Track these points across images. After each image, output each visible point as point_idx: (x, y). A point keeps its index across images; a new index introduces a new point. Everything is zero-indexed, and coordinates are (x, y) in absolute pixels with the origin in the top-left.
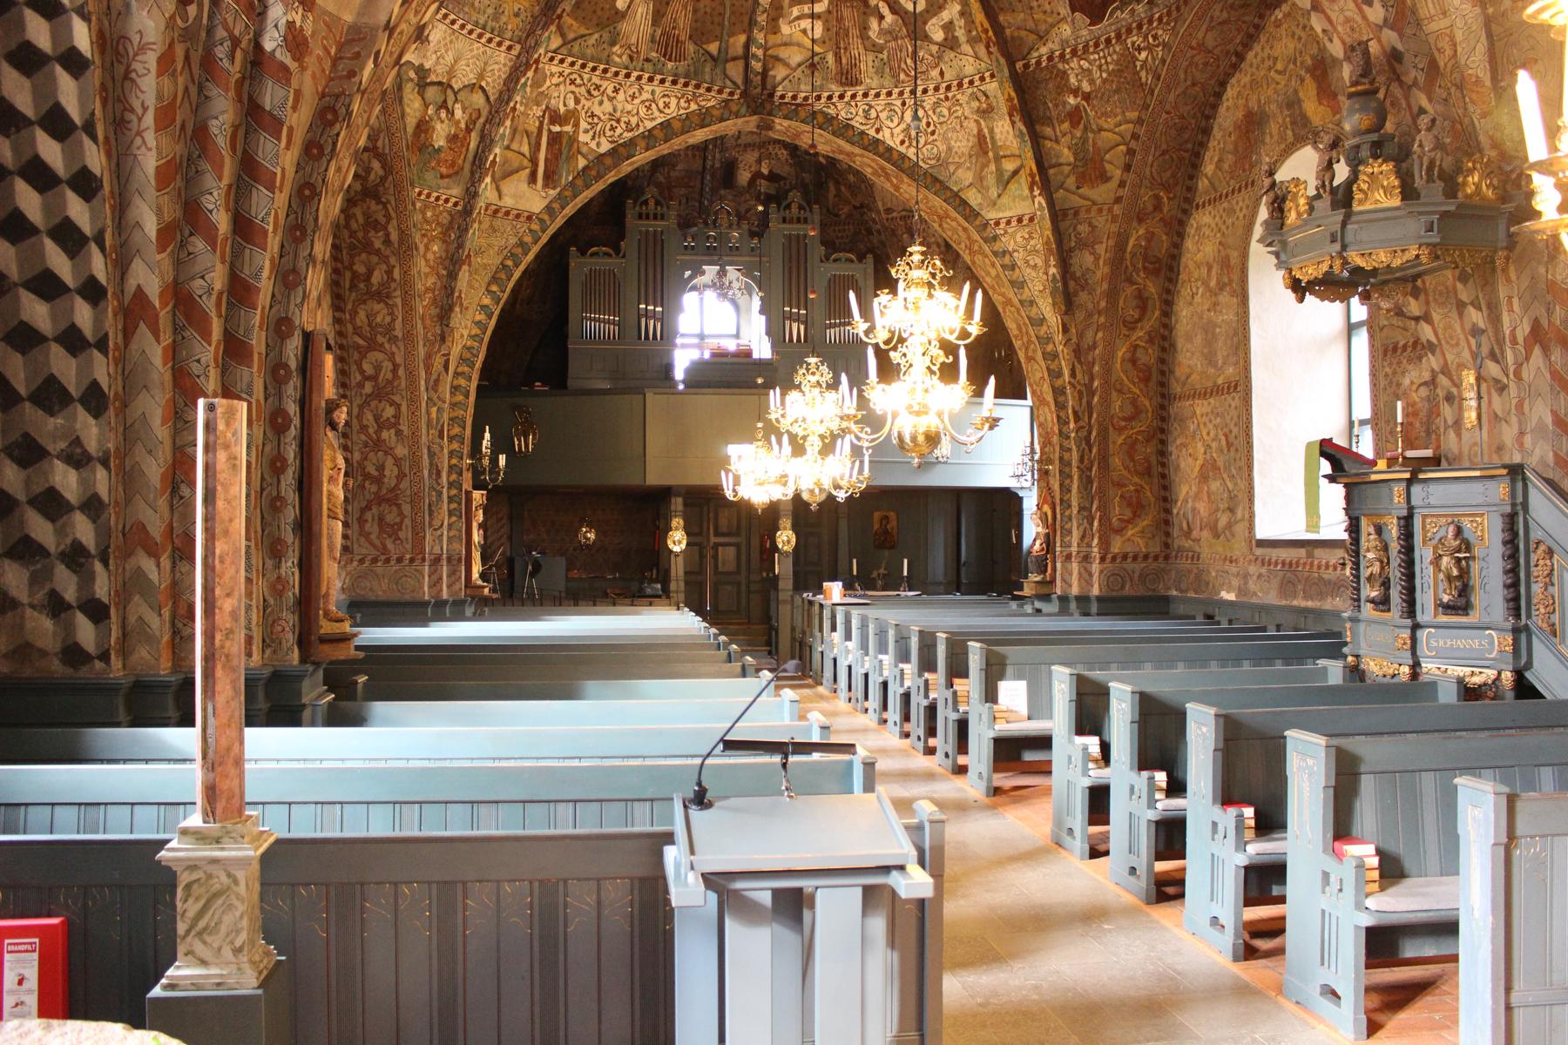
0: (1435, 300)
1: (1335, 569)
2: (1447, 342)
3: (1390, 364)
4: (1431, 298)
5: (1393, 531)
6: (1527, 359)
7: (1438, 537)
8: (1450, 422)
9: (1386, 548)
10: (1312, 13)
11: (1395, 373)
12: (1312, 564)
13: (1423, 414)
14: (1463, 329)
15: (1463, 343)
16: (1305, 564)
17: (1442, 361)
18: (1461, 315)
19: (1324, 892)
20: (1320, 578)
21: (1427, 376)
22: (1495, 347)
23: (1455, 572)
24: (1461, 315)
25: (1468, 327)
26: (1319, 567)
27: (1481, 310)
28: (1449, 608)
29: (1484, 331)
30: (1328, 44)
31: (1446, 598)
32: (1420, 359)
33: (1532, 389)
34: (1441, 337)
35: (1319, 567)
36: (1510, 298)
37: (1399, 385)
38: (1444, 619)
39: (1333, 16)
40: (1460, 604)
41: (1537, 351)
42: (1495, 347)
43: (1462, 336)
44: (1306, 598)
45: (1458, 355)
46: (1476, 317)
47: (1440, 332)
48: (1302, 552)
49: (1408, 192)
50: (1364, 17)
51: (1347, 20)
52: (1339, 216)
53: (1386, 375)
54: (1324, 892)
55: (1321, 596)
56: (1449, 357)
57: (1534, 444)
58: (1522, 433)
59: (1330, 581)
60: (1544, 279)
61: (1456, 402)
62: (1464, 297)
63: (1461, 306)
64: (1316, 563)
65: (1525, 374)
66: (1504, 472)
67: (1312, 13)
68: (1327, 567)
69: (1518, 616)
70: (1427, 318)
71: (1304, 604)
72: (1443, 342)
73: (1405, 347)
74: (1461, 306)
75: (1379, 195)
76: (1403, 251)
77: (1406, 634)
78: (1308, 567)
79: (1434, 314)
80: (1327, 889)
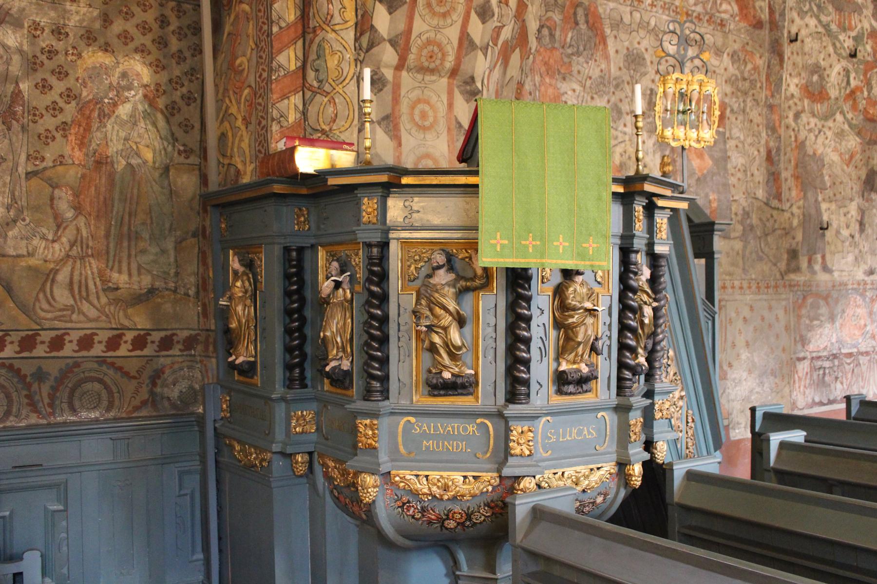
15: (457, 17)
45: (437, 29)
56: (419, 26)
61: (388, 89)
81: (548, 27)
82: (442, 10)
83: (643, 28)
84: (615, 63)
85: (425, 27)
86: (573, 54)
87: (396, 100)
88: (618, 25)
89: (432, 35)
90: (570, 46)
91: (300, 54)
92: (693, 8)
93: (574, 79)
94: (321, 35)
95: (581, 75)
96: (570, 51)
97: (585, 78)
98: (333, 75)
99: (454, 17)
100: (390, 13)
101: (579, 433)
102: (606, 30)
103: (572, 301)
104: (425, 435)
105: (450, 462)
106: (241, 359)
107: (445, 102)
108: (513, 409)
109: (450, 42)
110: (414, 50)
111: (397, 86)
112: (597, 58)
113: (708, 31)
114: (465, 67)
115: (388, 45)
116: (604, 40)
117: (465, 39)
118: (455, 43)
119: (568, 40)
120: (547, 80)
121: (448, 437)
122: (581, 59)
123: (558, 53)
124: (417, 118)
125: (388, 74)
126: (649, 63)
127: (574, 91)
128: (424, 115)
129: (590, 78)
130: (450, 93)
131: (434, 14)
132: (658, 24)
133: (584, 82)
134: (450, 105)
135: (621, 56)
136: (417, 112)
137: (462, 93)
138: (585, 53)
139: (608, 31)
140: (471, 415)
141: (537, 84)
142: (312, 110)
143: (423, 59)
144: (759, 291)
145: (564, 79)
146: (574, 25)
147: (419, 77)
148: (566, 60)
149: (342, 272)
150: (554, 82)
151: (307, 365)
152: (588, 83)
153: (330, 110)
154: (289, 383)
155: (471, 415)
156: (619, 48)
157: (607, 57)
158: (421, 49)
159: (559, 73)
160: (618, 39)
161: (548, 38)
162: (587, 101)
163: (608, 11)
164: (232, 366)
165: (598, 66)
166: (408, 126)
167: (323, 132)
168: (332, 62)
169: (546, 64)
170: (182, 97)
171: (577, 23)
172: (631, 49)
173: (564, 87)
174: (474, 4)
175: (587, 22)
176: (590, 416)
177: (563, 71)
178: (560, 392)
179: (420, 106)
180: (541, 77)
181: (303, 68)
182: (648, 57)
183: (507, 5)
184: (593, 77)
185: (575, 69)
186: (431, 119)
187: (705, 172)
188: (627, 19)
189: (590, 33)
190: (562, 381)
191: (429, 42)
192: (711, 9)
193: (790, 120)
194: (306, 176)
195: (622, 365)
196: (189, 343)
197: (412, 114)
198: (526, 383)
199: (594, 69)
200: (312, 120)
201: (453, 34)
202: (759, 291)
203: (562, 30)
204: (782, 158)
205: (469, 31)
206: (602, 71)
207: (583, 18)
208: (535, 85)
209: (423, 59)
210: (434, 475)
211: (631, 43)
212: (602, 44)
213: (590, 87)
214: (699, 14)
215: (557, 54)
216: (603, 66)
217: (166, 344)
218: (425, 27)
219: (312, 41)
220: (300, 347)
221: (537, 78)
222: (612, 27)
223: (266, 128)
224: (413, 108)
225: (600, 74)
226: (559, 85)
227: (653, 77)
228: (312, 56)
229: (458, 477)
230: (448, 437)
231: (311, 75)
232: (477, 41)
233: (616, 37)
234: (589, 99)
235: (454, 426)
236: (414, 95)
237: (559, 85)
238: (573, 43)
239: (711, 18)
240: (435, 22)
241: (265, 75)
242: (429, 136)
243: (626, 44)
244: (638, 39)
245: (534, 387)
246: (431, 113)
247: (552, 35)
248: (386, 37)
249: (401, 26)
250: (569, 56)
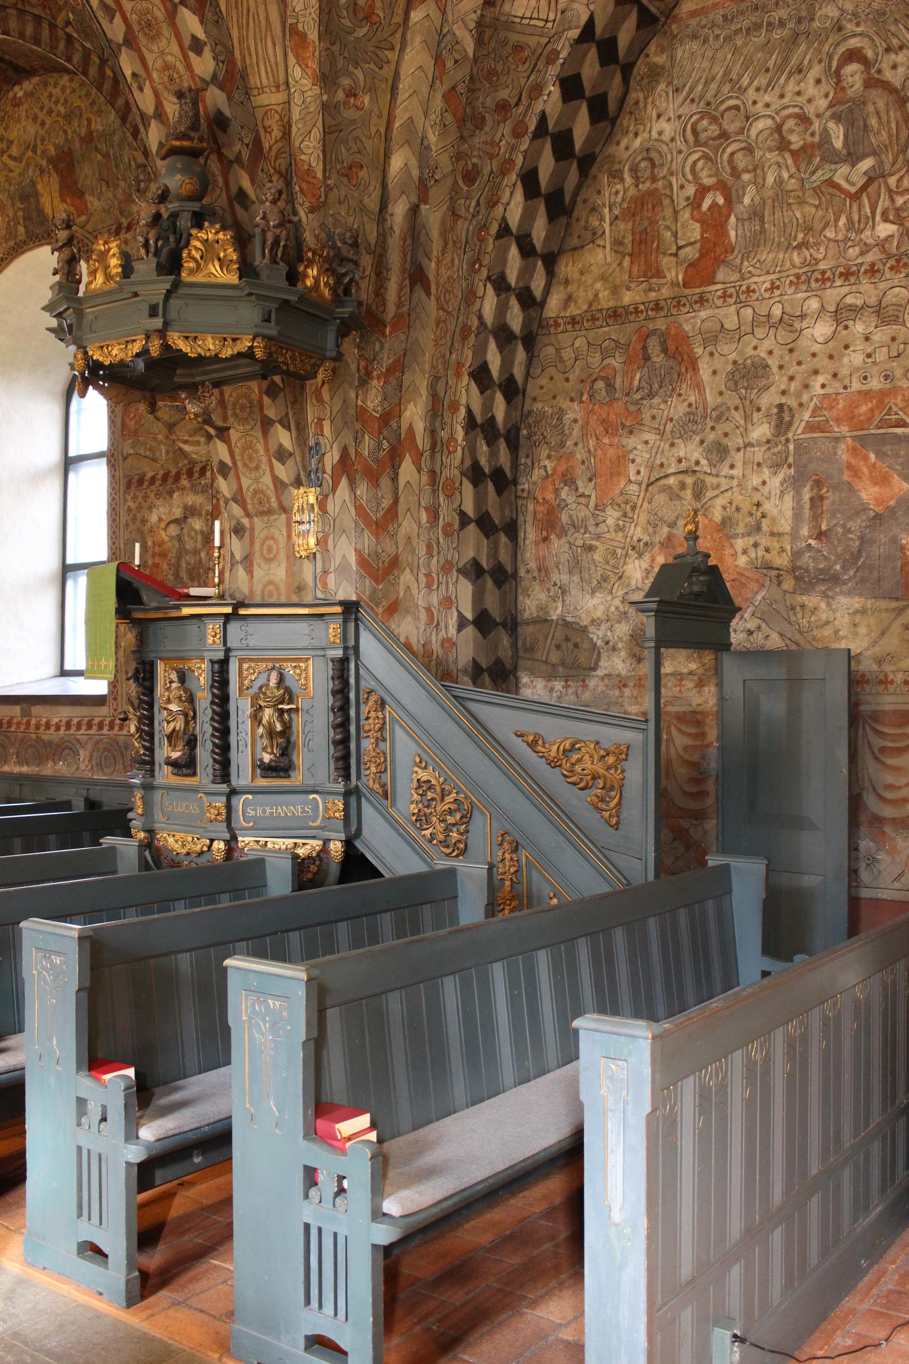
0: (235, 415)
1: (58, 728)
2: (245, 465)
3: (135, 498)
4: (230, 413)
5: (202, 676)
6: (334, 490)
7: (257, 685)
8: (238, 557)
9: (191, 699)
10: (123, 49)
11: (140, 507)
12: (28, 724)
13: (172, 555)
14: (267, 450)
15: (265, 466)
16: (19, 723)
17: (235, 487)
18: (265, 433)
19: (306, 1196)
20: (39, 739)
21: (178, 513)
22: (302, 473)
23: (279, 727)
24: (265, 433)
25: (273, 448)
26: (38, 727)
27: (289, 430)
28: (269, 770)
29: (291, 454)
30: (136, 93)
31: (267, 758)
32: (170, 493)
33: (337, 523)
34: (238, 458)
35: (38, 727)
36: (321, 420)
37: (144, 521)
38: (262, 782)
39: (149, 58)
40: (186, 766)
41: (344, 483)
42: (302, 473)
43: (264, 459)
44: (20, 763)
45: (257, 480)
46: (284, 438)
47: (237, 451)
48: (16, 710)
49: (246, 269)
50: (189, 67)
51: (167, 67)
52: (165, 284)
53: (129, 510)
54: (306, 1196)
55: (40, 760)
56: (245, 482)
57: (338, 585)
58: (326, 572)
59: (50, 744)
60: (354, 404)
61: (247, 535)
62: (271, 413)
63: (266, 424)
64: (33, 722)
65: (330, 507)
66: (338, 609)
67: (123, 49)
68: (48, 726)
69: (347, 777)
71: (17, 769)
72: (239, 464)
73: (153, 480)
74: (266, 424)
75: (214, 268)
76: (234, 340)
77: (220, 802)
78: (23, 727)
80: (313, 1192)
81: (602, 378)
83: (760, 325)
84: (711, 389)
85: (250, 482)
86: (642, 399)
87: (252, 542)
88: (717, 336)
89: (255, 486)
92: (859, 261)
93: (646, 428)
95: (658, 420)
96: (638, 396)
97: (663, 421)
99: (263, 467)
101: (187, 807)
102: (695, 350)
109: (268, 488)
110: (249, 501)
111: (252, 529)
112: (683, 392)
113: (896, 282)
116: (693, 364)
117: (276, 480)
118: (272, 486)
119: (636, 383)
120: (606, 441)
122: (656, 401)
123: (620, 403)
124: (265, 552)
125: (592, 449)
127: (646, 443)
128: (270, 550)
129: (671, 420)
132: (788, 309)
133: (662, 428)
135: (722, 377)
136: (265, 547)
138: (662, 391)
139: (699, 350)
145: (631, 432)
146: (642, 362)
147: (266, 518)
148: (632, 408)
150: (615, 440)
152: (669, 426)
156: (718, 366)
157: (699, 387)
158: (253, 498)
159: (623, 426)
161: (603, 392)
162: (663, 452)
165: (684, 400)
166: (259, 561)
169: (603, 421)
171: (647, 358)
172: (740, 362)
173: (632, 442)
174: (271, 453)
175: (665, 351)
177: (628, 424)
179: (268, 542)
180: (597, 439)
182: (773, 363)
184: (675, 418)
185: (646, 416)
186: (274, 551)
188: (731, 323)
189: (671, 363)
191: (256, 492)
192: (898, 248)
197: (262, 550)
199: (675, 407)
201: (267, 480)
203: (625, 373)
206: (690, 405)
207: (658, 348)
208: (589, 451)
211: (741, 353)
212: (690, 372)
213: (672, 432)
214: (873, 265)
215: (618, 406)
216: (692, 399)
218: (250, 482)
221: (592, 443)
222: (705, 344)
224: (262, 545)
225: (688, 410)
226: (625, 441)
227: (783, 387)
233: (711, 354)
234: (667, 447)
236: (262, 536)
237: (625, 441)
238: (644, 384)
239: (898, 261)
240: (253, 476)
242: (273, 566)
243: (732, 357)
244: (755, 342)
246: (275, 547)
247: (610, 385)
249: (235, 487)
250: (637, 403)
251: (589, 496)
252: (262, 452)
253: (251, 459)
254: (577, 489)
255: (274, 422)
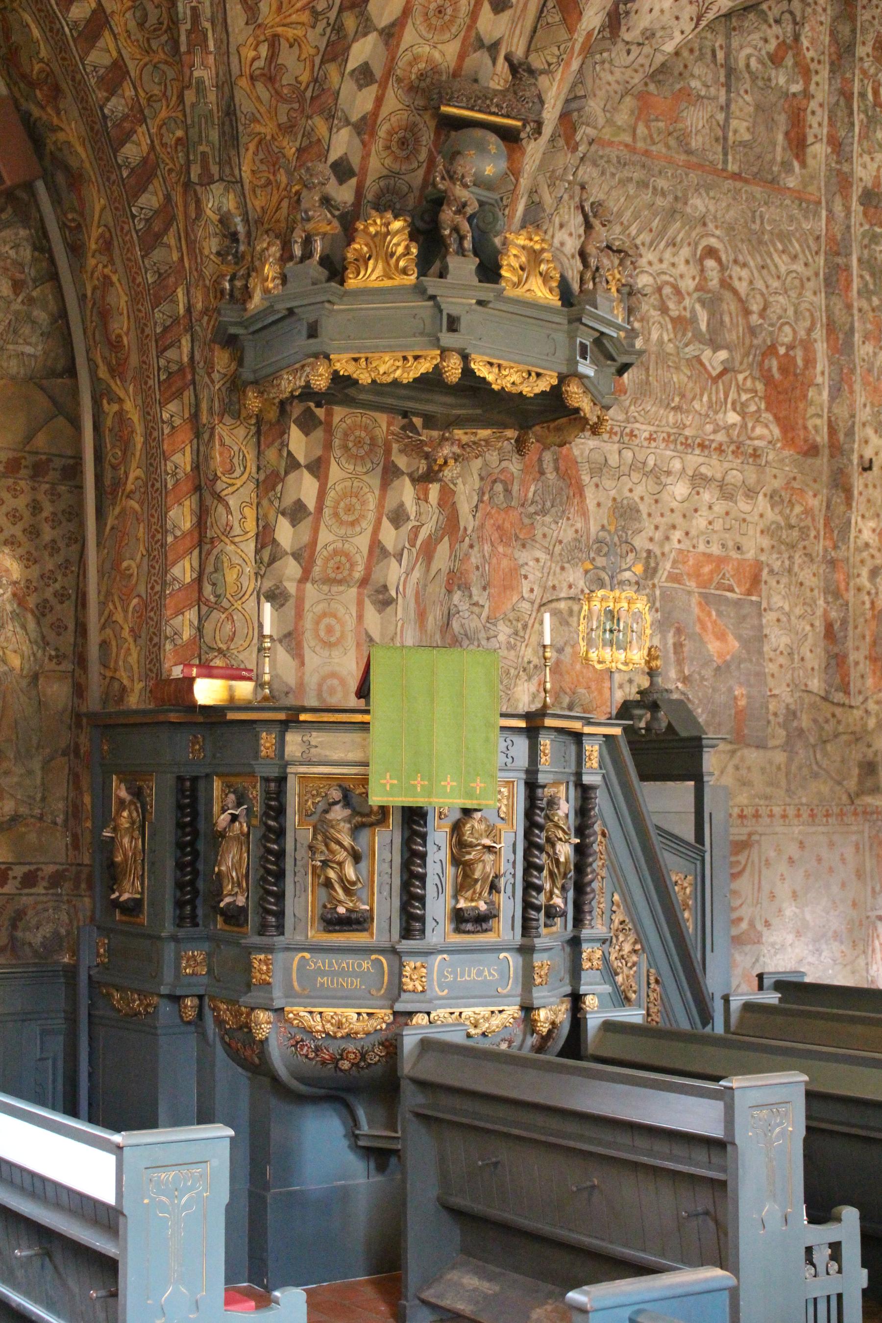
0: (345, 448)
2: (336, 515)
4: (337, 442)
14: (381, 505)
15: (367, 525)
18: (385, 485)
24: (385, 485)
25: (391, 503)
34: (329, 502)
43: (371, 516)
45: (344, 539)
47: (331, 495)
50: (474, 15)
56: (325, 536)
61: (291, 603)
62: (401, 461)
63: (390, 473)
70: (318, 468)
72: (327, 512)
74: (390, 473)
79: (334, 467)
81: (502, 481)
82: (351, 518)
83: (637, 470)
84: (595, 520)
85: (332, 538)
86: (535, 513)
87: (299, 614)
88: (601, 469)
89: (339, 545)
90: (532, 503)
91: (196, 564)
92: (712, 437)
93: (537, 545)
94: (220, 546)
95: (548, 539)
96: (532, 509)
97: (553, 542)
98: (231, 589)
99: (364, 524)
100: (294, 526)
101: (479, 973)
102: (583, 477)
103: (468, 838)
104: (321, 973)
105: (344, 999)
106: (126, 896)
107: (354, 614)
108: (406, 945)
109: (359, 551)
110: (319, 562)
113: (734, 466)
114: (377, 576)
115: (291, 558)
116: (580, 492)
118: (365, 550)
119: (530, 495)
120: (501, 549)
121: (343, 973)
122: (548, 519)
123: (515, 513)
124: (322, 634)
126: (645, 516)
127: (537, 560)
128: (330, 630)
129: (561, 542)
130: (360, 604)
131: (342, 523)
132: (658, 462)
133: (551, 548)
134: (360, 617)
135: (604, 511)
136: (322, 626)
137: (374, 603)
138: (553, 510)
139: (586, 478)
140: (366, 951)
141: (487, 555)
142: (208, 627)
143: (329, 571)
144: (813, 821)
145: (524, 546)
146: (538, 475)
147: (325, 588)
148: (527, 521)
149: (239, 804)
150: (509, 551)
151: (199, 902)
152: (558, 548)
153: (228, 626)
154: (180, 921)
155: (366, 951)
156: (602, 500)
157: (584, 514)
158: (327, 560)
159: (517, 538)
160: (601, 488)
161: (502, 496)
162: (555, 574)
163: (587, 452)
164: (116, 904)
165: (572, 525)
166: (312, 643)
167: (220, 651)
168: (231, 576)
169: (499, 528)
170: (55, 594)
171: (542, 473)
172: (619, 500)
173: (524, 556)
174: (386, 511)
175: (557, 469)
176: (491, 956)
177: (521, 536)
178: (458, 930)
179: (326, 621)
180: (493, 545)
181: (199, 580)
182: (644, 509)
183: (427, 501)
184: (565, 541)
185: (539, 533)
186: (338, 634)
187: (728, 657)
188: (613, 460)
189: (561, 484)
190: (460, 919)
191: (336, 552)
192: (738, 436)
193: (864, 580)
194: (205, 708)
195: (528, 905)
196: (56, 880)
197: (316, 631)
198: (422, 919)
199: (565, 530)
200: (208, 638)
201: (362, 542)
202: (813, 821)
203: (522, 482)
204: (850, 633)
205: (381, 537)
206: (577, 531)
207: (551, 465)
208: (484, 556)
209: (329, 571)
210: (329, 1011)
211: (620, 492)
212: (578, 496)
213: (560, 554)
214: (721, 445)
215: (514, 515)
216: (579, 525)
217: (29, 880)
218: (332, 538)
219: (209, 553)
220: (192, 883)
221: (487, 548)
222: (592, 473)
223: (159, 646)
224: (317, 623)
225: (575, 535)
226: (517, 554)
227: (651, 534)
228: (210, 568)
229: (352, 1013)
230: (343, 973)
231: (208, 589)
232: (390, 547)
233: (597, 486)
234: (558, 570)
235: (349, 962)
236: (319, 609)
237: (517, 554)
238: (537, 498)
239: (738, 448)
240: (342, 532)
241: (158, 588)
242: (335, 653)
243: (613, 493)
244: (630, 485)
245: (429, 924)
246: (337, 628)
247: (507, 491)
248: (289, 550)
249: (306, 538)
250: (530, 516)
251: (483, 606)
252: (372, 505)
253: (349, 509)
254: (470, 596)
255: (403, 473)
